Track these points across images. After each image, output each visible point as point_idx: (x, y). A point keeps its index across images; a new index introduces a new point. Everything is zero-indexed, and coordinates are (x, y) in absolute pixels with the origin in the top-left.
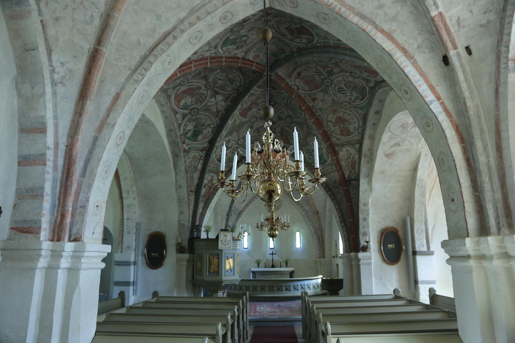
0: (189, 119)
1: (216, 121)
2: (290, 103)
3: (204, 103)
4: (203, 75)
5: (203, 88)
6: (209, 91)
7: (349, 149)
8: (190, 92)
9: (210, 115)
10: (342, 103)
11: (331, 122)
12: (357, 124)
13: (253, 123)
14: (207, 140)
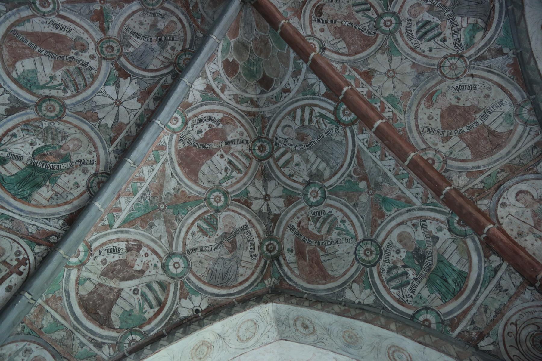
0: (27, 123)
1: (105, 154)
2: (310, 121)
3: (84, 95)
5: (92, 50)
6: (104, 63)
7: (523, 186)
9: (93, 134)
10: (440, 67)
11: (431, 130)
12: (507, 101)
13: (217, 211)
14: (65, 210)
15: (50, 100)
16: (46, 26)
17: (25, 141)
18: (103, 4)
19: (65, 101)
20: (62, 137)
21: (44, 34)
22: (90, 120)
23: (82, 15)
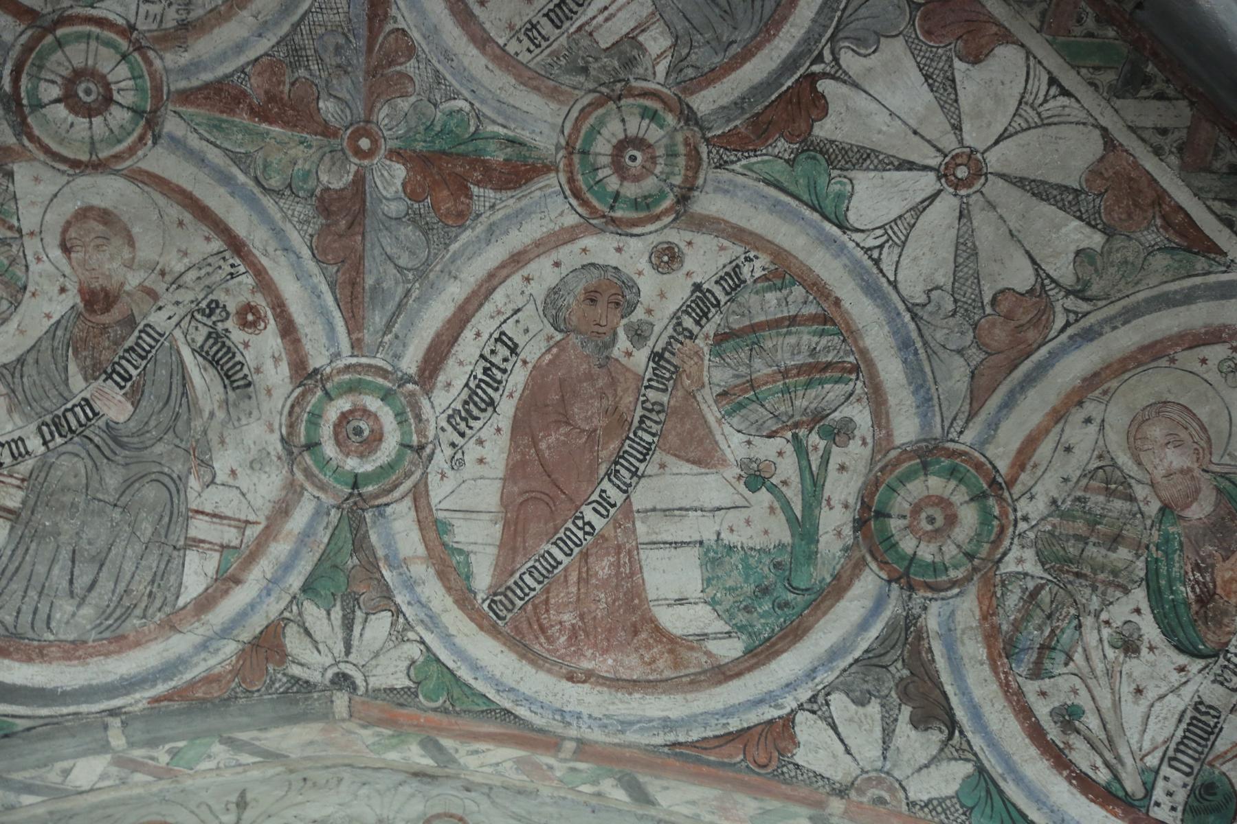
0: (1003, 648)
3: (878, 340)
4: (390, 178)
5: (630, 255)
6: (708, 203)
8: (583, 432)
9: (1126, 339)
15: (882, 515)
16: (472, 452)
17: (1109, 674)
18: (374, 142)
19: (898, 441)
20: (1110, 493)
21: (515, 471)
22: (1031, 335)
23: (427, 263)
